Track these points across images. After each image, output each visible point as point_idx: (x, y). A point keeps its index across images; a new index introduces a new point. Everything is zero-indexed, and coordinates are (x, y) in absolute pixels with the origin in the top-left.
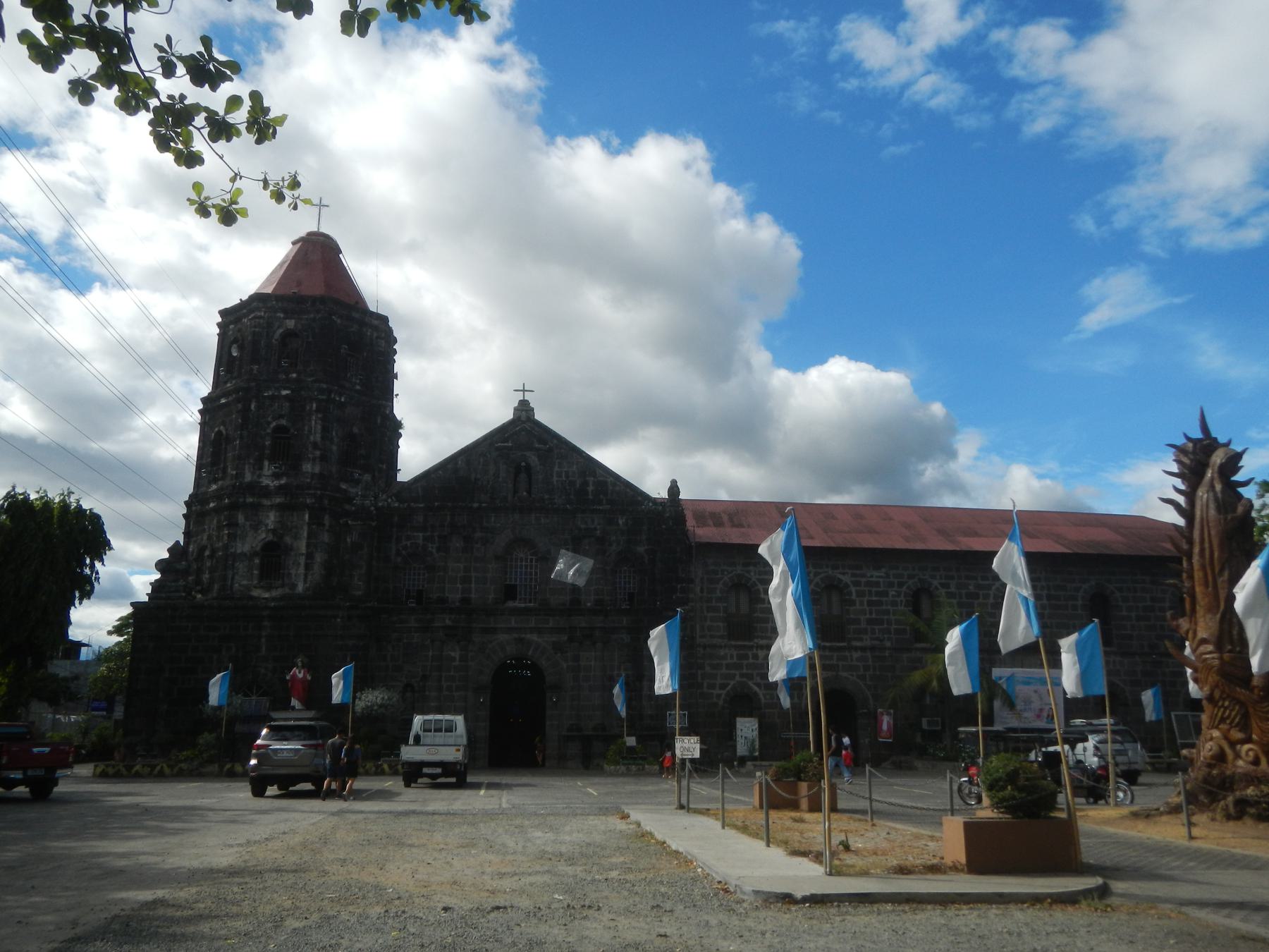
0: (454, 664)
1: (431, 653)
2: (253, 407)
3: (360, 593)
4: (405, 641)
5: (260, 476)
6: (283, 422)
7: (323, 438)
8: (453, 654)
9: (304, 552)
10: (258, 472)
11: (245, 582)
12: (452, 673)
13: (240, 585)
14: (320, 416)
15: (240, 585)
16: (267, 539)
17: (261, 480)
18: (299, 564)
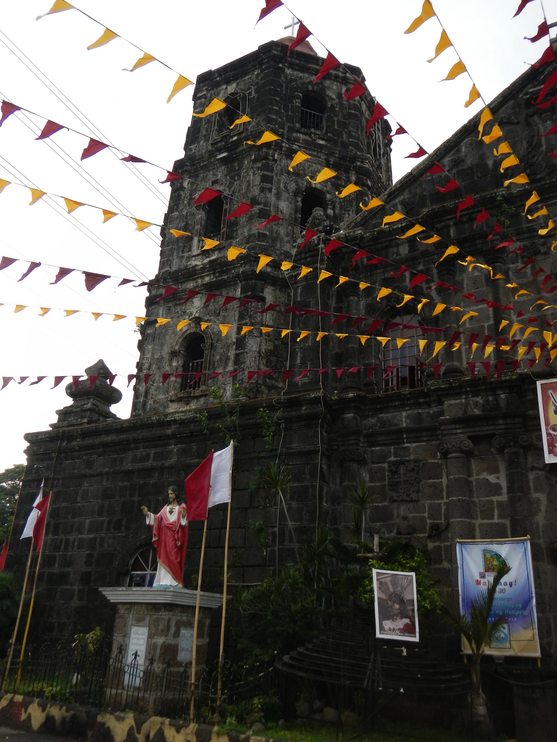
0: (495, 499)
1: (444, 480)
2: (185, 184)
3: (306, 380)
4: (392, 459)
5: (189, 258)
6: (217, 187)
7: (262, 190)
8: (492, 479)
9: (234, 340)
10: (186, 255)
11: (162, 397)
12: (496, 520)
13: (155, 401)
14: (259, 165)
15: (155, 401)
16: (189, 332)
17: (189, 263)
18: (228, 358)
